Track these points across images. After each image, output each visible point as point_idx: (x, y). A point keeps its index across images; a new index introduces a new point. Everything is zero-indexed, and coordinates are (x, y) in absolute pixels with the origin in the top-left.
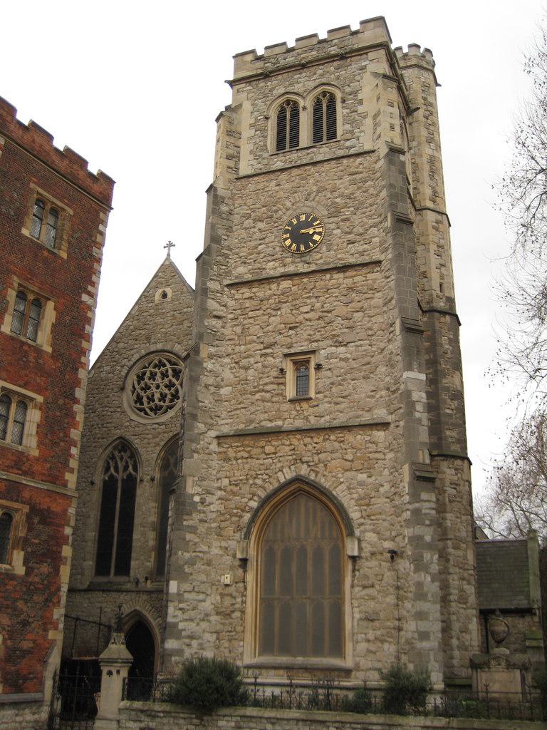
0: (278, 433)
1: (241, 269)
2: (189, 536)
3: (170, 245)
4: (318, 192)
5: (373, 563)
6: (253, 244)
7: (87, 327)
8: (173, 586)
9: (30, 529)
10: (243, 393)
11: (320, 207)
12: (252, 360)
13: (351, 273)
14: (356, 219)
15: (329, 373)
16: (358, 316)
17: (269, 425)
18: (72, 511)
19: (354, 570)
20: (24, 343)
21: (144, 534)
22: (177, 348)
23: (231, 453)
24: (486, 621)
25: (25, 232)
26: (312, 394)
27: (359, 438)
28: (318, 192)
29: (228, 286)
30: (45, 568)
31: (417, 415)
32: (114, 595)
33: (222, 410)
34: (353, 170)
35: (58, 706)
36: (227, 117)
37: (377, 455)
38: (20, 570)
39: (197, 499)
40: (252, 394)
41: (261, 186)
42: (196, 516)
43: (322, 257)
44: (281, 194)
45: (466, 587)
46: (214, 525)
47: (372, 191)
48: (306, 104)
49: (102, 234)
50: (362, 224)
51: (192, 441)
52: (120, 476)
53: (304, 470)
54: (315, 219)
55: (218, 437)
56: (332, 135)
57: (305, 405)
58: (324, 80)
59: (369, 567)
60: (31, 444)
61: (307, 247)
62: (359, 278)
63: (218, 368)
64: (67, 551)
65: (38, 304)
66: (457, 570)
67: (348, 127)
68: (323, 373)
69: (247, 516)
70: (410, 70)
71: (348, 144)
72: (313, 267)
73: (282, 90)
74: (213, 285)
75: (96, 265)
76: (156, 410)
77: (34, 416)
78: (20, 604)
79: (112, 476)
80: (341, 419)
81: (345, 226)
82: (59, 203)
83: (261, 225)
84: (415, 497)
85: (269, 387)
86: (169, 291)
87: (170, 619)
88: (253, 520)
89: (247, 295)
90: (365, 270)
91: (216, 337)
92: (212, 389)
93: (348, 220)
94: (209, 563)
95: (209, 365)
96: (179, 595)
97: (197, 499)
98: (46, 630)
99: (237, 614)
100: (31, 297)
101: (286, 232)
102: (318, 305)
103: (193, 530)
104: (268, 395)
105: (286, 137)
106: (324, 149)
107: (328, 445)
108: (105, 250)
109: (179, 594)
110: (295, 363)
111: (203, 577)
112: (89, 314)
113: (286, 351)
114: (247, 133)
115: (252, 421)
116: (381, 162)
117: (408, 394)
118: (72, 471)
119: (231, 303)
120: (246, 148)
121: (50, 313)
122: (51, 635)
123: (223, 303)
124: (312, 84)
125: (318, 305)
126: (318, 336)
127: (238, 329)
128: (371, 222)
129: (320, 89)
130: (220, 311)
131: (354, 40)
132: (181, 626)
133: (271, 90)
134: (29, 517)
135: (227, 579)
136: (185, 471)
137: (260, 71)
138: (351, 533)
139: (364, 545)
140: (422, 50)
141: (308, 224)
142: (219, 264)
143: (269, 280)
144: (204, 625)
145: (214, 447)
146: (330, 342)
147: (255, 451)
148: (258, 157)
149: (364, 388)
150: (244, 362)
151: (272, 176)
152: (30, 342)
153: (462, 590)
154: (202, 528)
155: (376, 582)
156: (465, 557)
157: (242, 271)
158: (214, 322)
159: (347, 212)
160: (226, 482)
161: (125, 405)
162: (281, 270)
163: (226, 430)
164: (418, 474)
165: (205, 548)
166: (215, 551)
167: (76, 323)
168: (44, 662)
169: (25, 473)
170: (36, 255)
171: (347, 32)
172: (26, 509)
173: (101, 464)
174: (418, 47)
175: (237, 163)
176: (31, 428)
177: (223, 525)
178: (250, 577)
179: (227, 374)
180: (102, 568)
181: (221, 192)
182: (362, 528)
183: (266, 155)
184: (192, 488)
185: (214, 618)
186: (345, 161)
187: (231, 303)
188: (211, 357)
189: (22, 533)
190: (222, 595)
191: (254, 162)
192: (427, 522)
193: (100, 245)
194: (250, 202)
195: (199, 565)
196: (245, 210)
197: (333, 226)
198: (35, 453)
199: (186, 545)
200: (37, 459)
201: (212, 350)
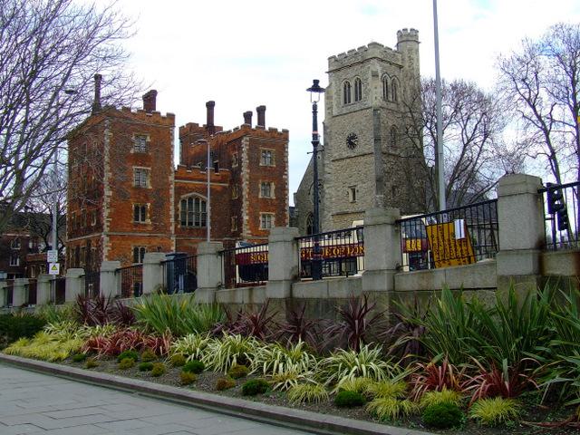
0: (347, 213)
1: (336, 154)
25: (261, 164)
65: (269, 185)
74: (326, 162)
77: (273, 219)
91: (328, 181)
95: (327, 191)
105: (347, 100)
114: (335, 97)
121: (273, 186)
157: (336, 155)
159: (364, 132)
167: (282, 188)
179: (333, 193)
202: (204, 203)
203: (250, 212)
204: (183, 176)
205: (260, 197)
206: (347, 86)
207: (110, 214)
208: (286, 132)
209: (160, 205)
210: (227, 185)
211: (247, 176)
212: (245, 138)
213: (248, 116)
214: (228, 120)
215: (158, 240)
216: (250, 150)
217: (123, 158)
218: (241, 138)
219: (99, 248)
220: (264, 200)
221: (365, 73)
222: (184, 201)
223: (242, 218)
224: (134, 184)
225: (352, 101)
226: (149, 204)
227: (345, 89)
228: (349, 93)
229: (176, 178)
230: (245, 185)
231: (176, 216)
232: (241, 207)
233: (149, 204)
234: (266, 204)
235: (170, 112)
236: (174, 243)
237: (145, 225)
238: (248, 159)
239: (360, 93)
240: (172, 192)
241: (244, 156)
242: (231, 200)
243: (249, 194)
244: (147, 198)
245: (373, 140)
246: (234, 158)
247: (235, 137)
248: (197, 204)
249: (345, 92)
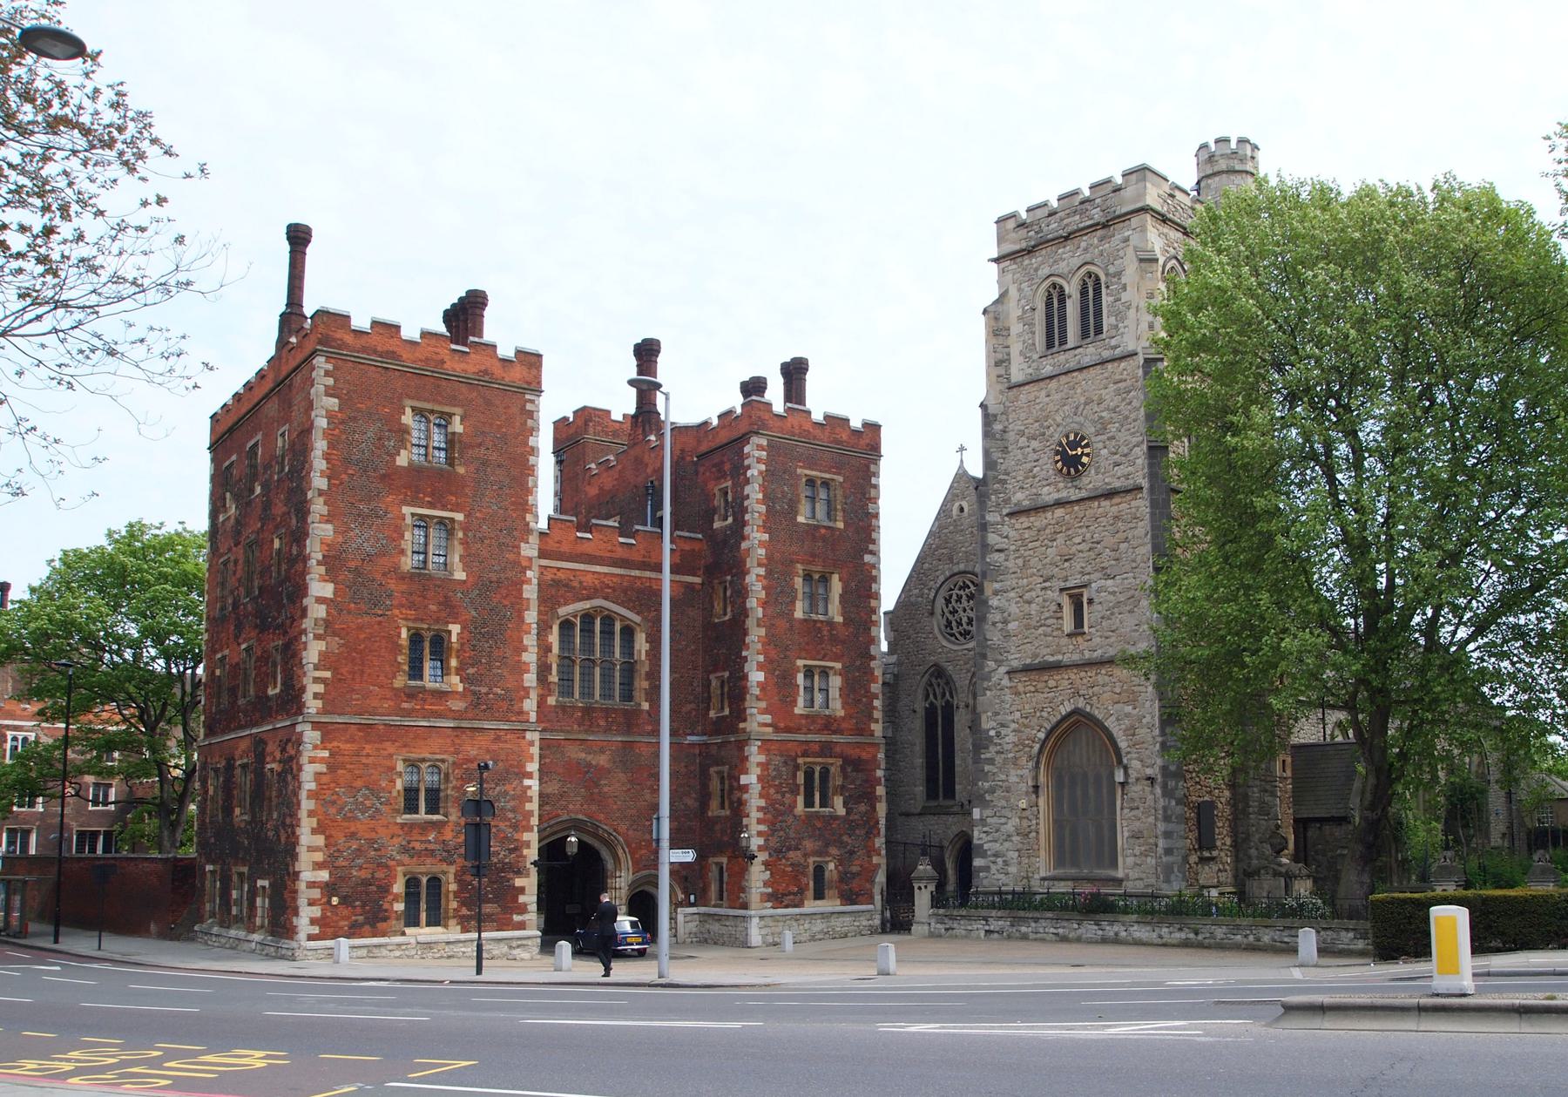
0: (1057, 667)
2: (987, 768)
3: (962, 449)
4: (1086, 404)
6: (1028, 466)
9: (845, 777)
10: (1028, 627)
11: (1087, 424)
12: (1033, 594)
13: (1116, 500)
14: (1123, 436)
15: (1099, 607)
16: (1123, 546)
17: (1051, 659)
18: (881, 756)
20: (815, 621)
21: (964, 760)
22: (978, 569)
23: (1021, 688)
25: (801, 519)
26: (1086, 629)
28: (1086, 404)
30: (863, 808)
32: (944, 818)
34: (1118, 377)
35: (888, 914)
36: (994, 314)
38: (841, 811)
39: (992, 733)
40: (1036, 628)
41: (1032, 397)
42: (993, 749)
43: (1092, 481)
44: (1051, 407)
47: (1135, 403)
49: (876, 487)
50: (1126, 443)
52: (939, 703)
53: (1081, 703)
55: (1008, 673)
56: (1099, 330)
57: (1080, 639)
58: (1088, 257)
60: (837, 708)
61: (1077, 471)
62: (1122, 506)
63: (1003, 603)
64: (881, 791)
65: (825, 579)
68: (1096, 607)
69: (1037, 747)
70: (1217, 179)
71: (1113, 342)
72: (1084, 494)
73: (1046, 271)
74: (990, 518)
76: (966, 634)
77: (836, 682)
78: (845, 838)
79: (932, 704)
80: (1111, 652)
82: (827, 476)
83: (1035, 444)
85: (1049, 622)
86: (965, 504)
87: (975, 841)
88: (1040, 751)
89: (1026, 525)
90: (1129, 497)
91: (997, 572)
92: (1000, 625)
93: (1113, 438)
95: (994, 602)
96: (983, 821)
98: (870, 857)
100: (816, 576)
101: (1057, 453)
102: (1088, 536)
103: (991, 761)
105: (1054, 337)
106: (1091, 349)
108: (881, 502)
110: (1071, 596)
111: (1004, 803)
112: (874, 572)
113: (1063, 585)
114: (1016, 328)
115: (1037, 656)
116: (1140, 372)
118: (877, 721)
119: (1012, 534)
120: (1016, 349)
121: (836, 586)
122: (875, 860)
123: (1004, 534)
124: (1076, 262)
125: (1088, 536)
126: (1089, 569)
127: (1020, 562)
128: (1135, 440)
129: (1083, 270)
131: (1114, 198)
133: (1036, 270)
134: (843, 768)
135: (1023, 804)
137: (1024, 245)
140: (1233, 145)
141: (1074, 445)
142: (996, 492)
143: (1044, 508)
145: (1006, 682)
146: (1099, 575)
147: (1040, 685)
148: (1028, 359)
149: (1130, 621)
150: (1027, 596)
151: (1042, 384)
152: (821, 617)
154: (999, 759)
157: (1020, 498)
158: (996, 556)
159: (1113, 428)
160: (1018, 714)
161: (936, 630)
162: (1056, 496)
163: (1015, 664)
165: (1003, 777)
166: (1013, 779)
167: (863, 585)
168: (872, 882)
169: (835, 732)
170: (814, 537)
172: (839, 762)
173: (920, 692)
174: (1227, 140)
175: (1007, 369)
176: (834, 693)
178: (1042, 802)
179: (1014, 609)
180: (932, 793)
181: (990, 411)
183: (1035, 356)
184: (987, 723)
185: (1016, 839)
186: (1109, 366)
187: (1012, 534)
188: (996, 593)
189: (839, 782)
191: (1025, 366)
193: (875, 500)
194: (1023, 416)
195: (999, 793)
197: (1100, 445)
198: (841, 713)
199: (985, 776)
200: (843, 718)
201: (997, 586)
202: (628, 632)
203: (769, 660)
204: (565, 548)
205: (799, 614)
206: (1055, 298)
207: (323, 656)
208: (873, 429)
209: (494, 630)
210: (697, 580)
211: (762, 552)
212: (755, 440)
213: (753, 387)
214: (696, 397)
215: (483, 740)
216: (768, 476)
217: (371, 480)
218: (743, 439)
219: (291, 768)
220: (809, 626)
221: (1115, 256)
222: (566, 626)
223: (745, 677)
224: (409, 562)
225: (1071, 343)
226: (455, 629)
227: (1049, 304)
228: (1063, 319)
229: (543, 554)
230: (755, 579)
231: (543, 670)
232: (742, 644)
233: (455, 629)
234: (815, 636)
235: (530, 346)
236: (535, 750)
237: (441, 695)
238: (764, 501)
239: (1098, 314)
240: (530, 592)
241: (754, 492)
242: (708, 626)
243: (764, 604)
244: (450, 610)
245: (1140, 452)
246: (718, 502)
247: (724, 437)
248: (608, 633)
249: (1049, 317)
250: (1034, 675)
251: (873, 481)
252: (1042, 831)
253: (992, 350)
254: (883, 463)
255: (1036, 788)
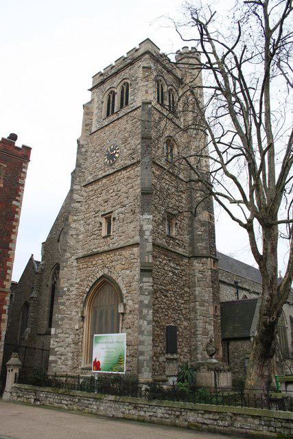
0: (97, 254)
2: (61, 307)
5: (131, 316)
7: (16, 216)
8: (53, 331)
10: (87, 236)
12: (91, 220)
13: (128, 170)
18: (8, 298)
19: (123, 320)
24: (228, 344)
27: (126, 253)
29: (84, 186)
31: (146, 237)
33: (79, 246)
37: (134, 261)
39: (65, 289)
43: (117, 166)
45: (208, 327)
46: (74, 301)
48: (118, 91)
49: (25, 173)
51: (63, 262)
53: (106, 271)
54: (117, 146)
55: (76, 259)
56: (127, 104)
57: (108, 239)
59: (129, 318)
66: (202, 317)
67: (132, 97)
75: (21, 187)
80: (122, 244)
81: (127, 146)
83: (98, 154)
84: (141, 281)
89: (90, 189)
92: (75, 236)
94: (71, 319)
95: (73, 225)
96: (56, 336)
97: (65, 289)
99: (80, 343)
101: (106, 155)
102: (116, 188)
103: (63, 304)
104: (95, 236)
105: (110, 111)
107: (115, 257)
109: (55, 334)
114: (95, 111)
117: (141, 226)
130: (80, 199)
132: (56, 349)
136: (60, 276)
138: (122, 301)
139: (127, 307)
140: (190, 49)
143: (98, 180)
144: (68, 349)
145: (75, 264)
147: (90, 264)
153: (205, 328)
154: (68, 303)
155: (131, 326)
156: (207, 311)
157: (90, 178)
158: (77, 204)
163: (80, 255)
164: (142, 268)
171: (134, 51)
173: (50, 278)
175: (91, 127)
177: (77, 300)
178: (85, 325)
179: (82, 229)
182: (127, 298)
187: (85, 194)
188: (74, 221)
190: (75, 334)
192: (146, 293)
193: (24, 178)
196: (92, 149)
201: (75, 218)
250: (87, 259)
251: (24, 170)
252: (84, 342)
253: (85, 120)
254: (30, 165)
255: (83, 317)
